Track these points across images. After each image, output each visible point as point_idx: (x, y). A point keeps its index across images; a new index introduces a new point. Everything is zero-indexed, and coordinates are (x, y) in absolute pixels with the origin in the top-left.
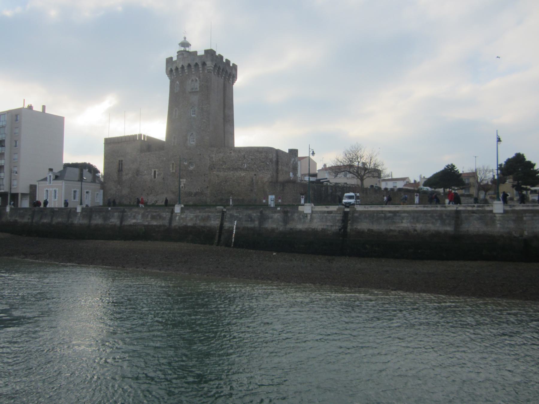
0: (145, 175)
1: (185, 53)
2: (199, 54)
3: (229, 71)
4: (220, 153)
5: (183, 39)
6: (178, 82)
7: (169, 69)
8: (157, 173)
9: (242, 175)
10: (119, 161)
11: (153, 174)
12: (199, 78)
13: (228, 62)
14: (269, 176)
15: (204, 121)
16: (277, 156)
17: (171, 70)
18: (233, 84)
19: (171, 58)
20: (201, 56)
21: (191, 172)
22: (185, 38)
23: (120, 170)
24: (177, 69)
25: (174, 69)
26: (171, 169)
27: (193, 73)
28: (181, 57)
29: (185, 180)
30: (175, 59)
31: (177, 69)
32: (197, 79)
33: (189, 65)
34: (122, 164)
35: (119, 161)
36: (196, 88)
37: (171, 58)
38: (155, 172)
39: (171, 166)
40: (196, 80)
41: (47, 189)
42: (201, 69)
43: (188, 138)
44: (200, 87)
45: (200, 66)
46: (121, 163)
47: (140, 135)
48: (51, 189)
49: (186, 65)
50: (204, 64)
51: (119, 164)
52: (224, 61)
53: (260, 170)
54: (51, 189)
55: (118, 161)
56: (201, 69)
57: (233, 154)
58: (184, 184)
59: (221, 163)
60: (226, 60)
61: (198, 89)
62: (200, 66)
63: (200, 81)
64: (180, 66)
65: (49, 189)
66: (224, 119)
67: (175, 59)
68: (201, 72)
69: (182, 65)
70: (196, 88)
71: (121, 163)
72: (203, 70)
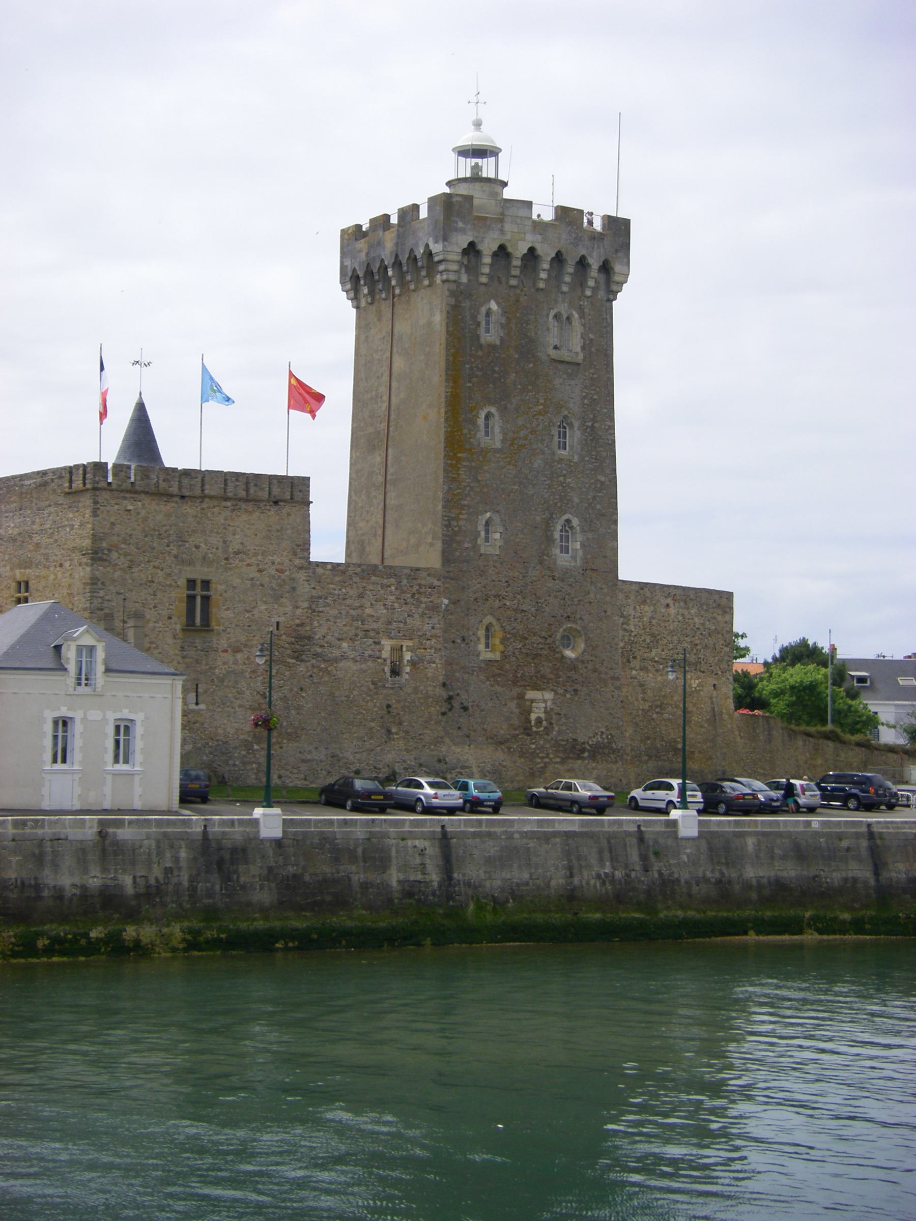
0: (344, 657)
8: (407, 656)
10: (191, 583)
17: (472, 250)
21: (573, 666)
24: (502, 252)
25: (488, 247)
26: (481, 647)
29: (549, 695)
31: (502, 252)
33: (559, 259)
34: (206, 599)
35: (191, 583)
39: (481, 633)
49: (546, 253)
51: (191, 599)
55: (182, 582)
57: (672, 611)
62: (594, 272)
64: (523, 249)
65: (78, 715)
69: (532, 250)
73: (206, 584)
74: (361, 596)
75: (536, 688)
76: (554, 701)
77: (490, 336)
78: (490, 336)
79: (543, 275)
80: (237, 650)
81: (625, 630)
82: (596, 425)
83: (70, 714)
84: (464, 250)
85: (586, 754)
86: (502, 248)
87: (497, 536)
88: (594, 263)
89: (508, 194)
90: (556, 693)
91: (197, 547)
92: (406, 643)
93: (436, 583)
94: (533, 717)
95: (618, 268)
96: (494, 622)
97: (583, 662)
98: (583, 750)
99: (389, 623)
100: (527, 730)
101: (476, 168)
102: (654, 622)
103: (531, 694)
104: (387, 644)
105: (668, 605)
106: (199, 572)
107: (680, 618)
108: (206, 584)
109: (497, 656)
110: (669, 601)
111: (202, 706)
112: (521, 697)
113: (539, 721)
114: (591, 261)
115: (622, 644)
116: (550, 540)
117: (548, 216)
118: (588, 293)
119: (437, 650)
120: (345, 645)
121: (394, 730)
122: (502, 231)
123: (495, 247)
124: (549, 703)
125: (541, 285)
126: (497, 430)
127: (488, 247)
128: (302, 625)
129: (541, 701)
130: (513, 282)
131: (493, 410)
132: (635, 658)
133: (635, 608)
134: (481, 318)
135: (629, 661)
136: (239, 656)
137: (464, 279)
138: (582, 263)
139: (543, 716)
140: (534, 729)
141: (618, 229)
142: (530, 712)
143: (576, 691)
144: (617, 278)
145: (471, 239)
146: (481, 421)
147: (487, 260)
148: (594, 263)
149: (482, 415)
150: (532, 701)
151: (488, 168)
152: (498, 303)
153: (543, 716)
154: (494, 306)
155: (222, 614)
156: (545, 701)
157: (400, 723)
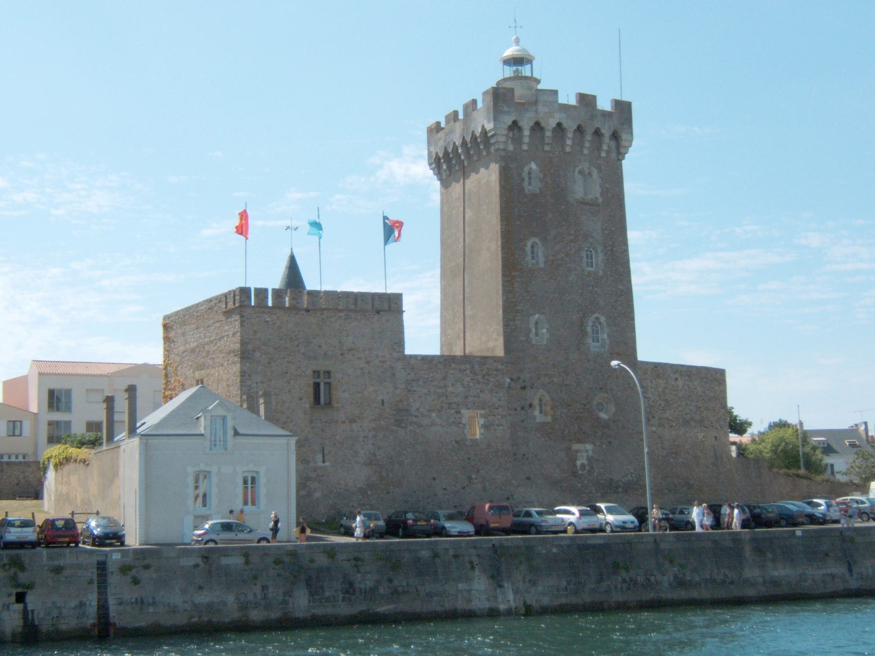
0: (433, 424)
10: (316, 373)
17: (515, 126)
24: (537, 127)
25: (526, 125)
26: (537, 413)
27: (586, 152)
29: (589, 447)
31: (537, 127)
33: (580, 130)
34: (329, 384)
35: (316, 373)
49: (570, 126)
51: (317, 386)
55: (309, 372)
57: (680, 383)
58: (588, 459)
64: (552, 123)
65: (214, 469)
69: (559, 125)
73: (328, 373)
74: (445, 378)
75: (580, 441)
76: (593, 451)
77: (532, 187)
78: (532, 187)
79: (569, 142)
80: (352, 421)
83: (207, 469)
84: (510, 127)
85: (620, 489)
86: (537, 124)
87: (545, 331)
88: (606, 132)
89: (540, 87)
90: (595, 445)
91: (320, 346)
93: (500, 367)
94: (579, 463)
95: (624, 136)
96: (545, 394)
97: (614, 421)
98: (618, 487)
99: (466, 397)
100: (575, 474)
102: (667, 391)
103: (576, 446)
105: (676, 379)
106: (322, 365)
107: (686, 388)
108: (328, 373)
109: (549, 419)
110: (677, 376)
111: (327, 464)
112: (569, 449)
113: (583, 466)
114: (603, 131)
116: (583, 333)
117: (573, 101)
118: (603, 155)
119: (503, 417)
120: (434, 415)
121: (473, 476)
122: (537, 112)
123: (532, 124)
124: (590, 453)
125: (568, 149)
126: (540, 254)
127: (526, 125)
128: (401, 401)
129: (584, 451)
130: (547, 148)
131: (537, 240)
132: (653, 417)
133: (651, 381)
134: (525, 175)
136: (354, 425)
137: (511, 148)
138: (597, 133)
139: (585, 462)
140: (580, 472)
141: (623, 109)
142: (575, 460)
143: (610, 443)
144: (624, 143)
145: (514, 119)
146: (528, 249)
147: (527, 133)
148: (606, 132)
149: (529, 244)
150: (577, 451)
151: (526, 71)
152: (536, 164)
153: (585, 462)
154: (533, 166)
155: (341, 395)
156: (587, 451)
157: (478, 471)
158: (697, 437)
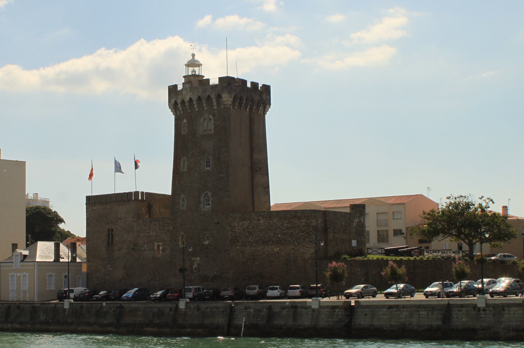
1: (195, 82)
2: (211, 83)
3: (257, 98)
4: (245, 220)
5: (191, 58)
6: (185, 121)
7: (173, 101)
8: (161, 248)
9: (276, 250)
10: (109, 230)
11: (156, 248)
12: (214, 116)
13: (255, 85)
14: (313, 250)
15: (222, 176)
16: (325, 221)
17: (176, 103)
18: (264, 114)
19: (176, 86)
20: (215, 86)
22: (193, 55)
23: (110, 243)
24: (183, 102)
25: (179, 101)
26: (180, 243)
27: (206, 108)
28: (188, 86)
29: (198, 259)
30: (180, 87)
31: (183, 102)
32: (211, 117)
33: (199, 98)
34: (112, 234)
36: (211, 130)
37: (176, 86)
38: (158, 246)
39: (180, 238)
40: (210, 119)
41: (13, 274)
42: (215, 104)
43: (202, 200)
44: (214, 128)
45: (214, 100)
46: (110, 234)
47: (137, 193)
48: (19, 274)
49: (195, 98)
50: (219, 97)
51: (109, 235)
52: (249, 85)
53: (299, 243)
54: (19, 274)
55: (106, 230)
56: (215, 104)
57: (262, 222)
58: (198, 265)
59: (247, 234)
60: (252, 83)
61: (213, 131)
62: (214, 100)
63: (215, 120)
64: (187, 99)
65: (15, 274)
66: (252, 168)
67: (180, 87)
68: (216, 108)
69: (190, 98)
70: (211, 130)
71: (110, 234)
72: (219, 104)
74: (150, 229)
76: (200, 261)
78: (184, 133)
79: (205, 105)
80: (120, 250)
81: (232, 232)
82: (220, 156)
85: (209, 280)
88: (213, 97)
92: (161, 244)
93: (169, 222)
94: (194, 267)
101: (194, 71)
102: (250, 227)
103: (193, 259)
104: (156, 244)
107: (267, 224)
108: (112, 230)
110: (260, 218)
113: (196, 268)
115: (230, 237)
116: (199, 202)
123: (180, 101)
133: (238, 223)
135: (234, 243)
136: (120, 252)
139: (196, 266)
142: (193, 265)
143: (207, 256)
150: (194, 261)
153: (196, 266)
156: (197, 261)
158: (273, 250)
